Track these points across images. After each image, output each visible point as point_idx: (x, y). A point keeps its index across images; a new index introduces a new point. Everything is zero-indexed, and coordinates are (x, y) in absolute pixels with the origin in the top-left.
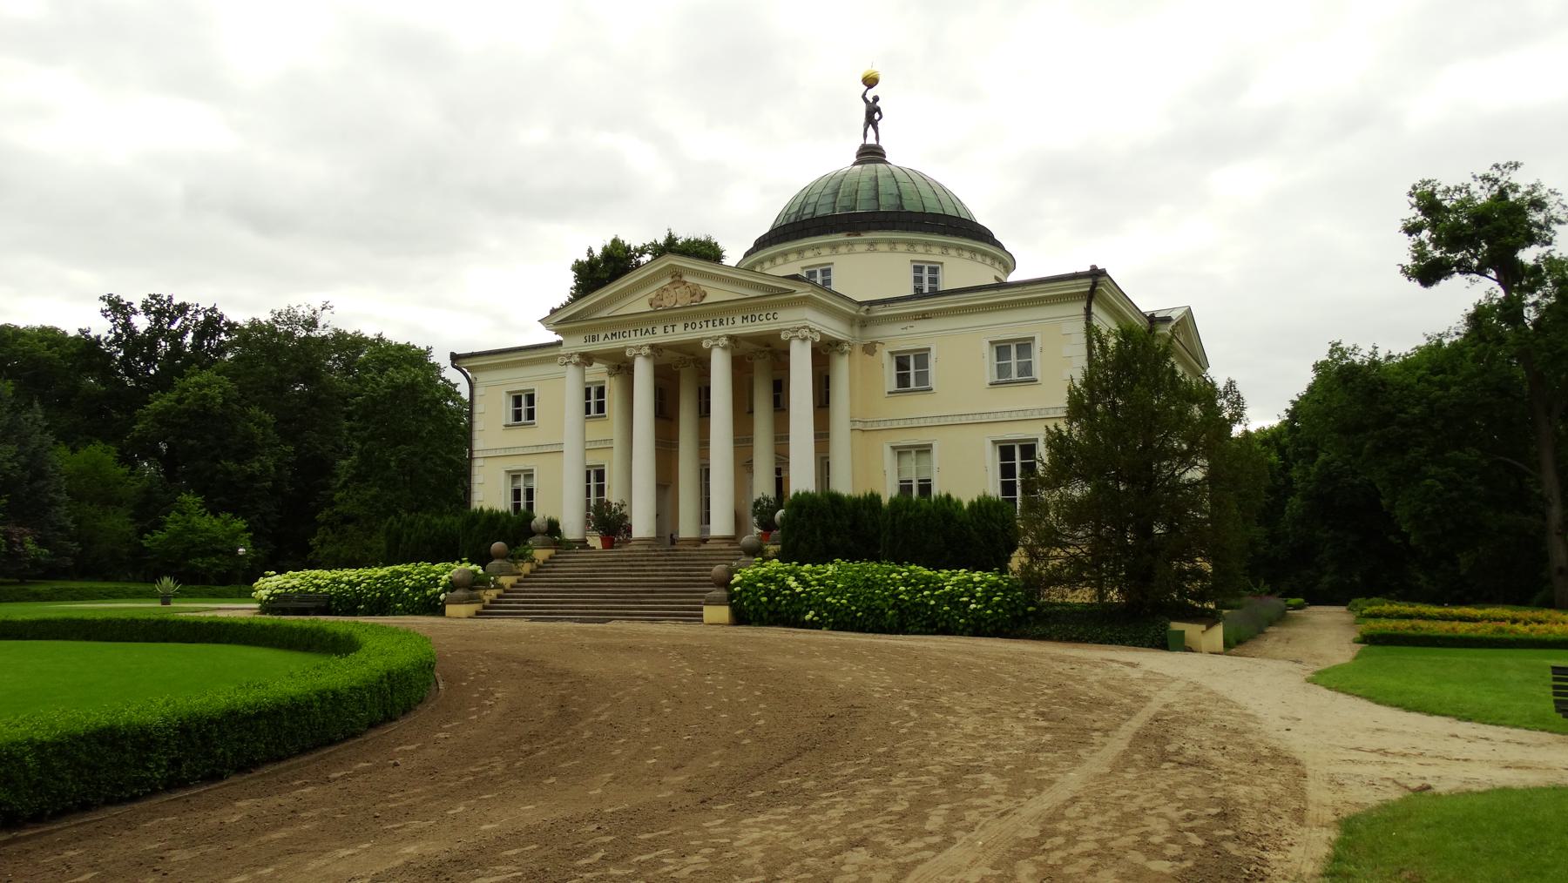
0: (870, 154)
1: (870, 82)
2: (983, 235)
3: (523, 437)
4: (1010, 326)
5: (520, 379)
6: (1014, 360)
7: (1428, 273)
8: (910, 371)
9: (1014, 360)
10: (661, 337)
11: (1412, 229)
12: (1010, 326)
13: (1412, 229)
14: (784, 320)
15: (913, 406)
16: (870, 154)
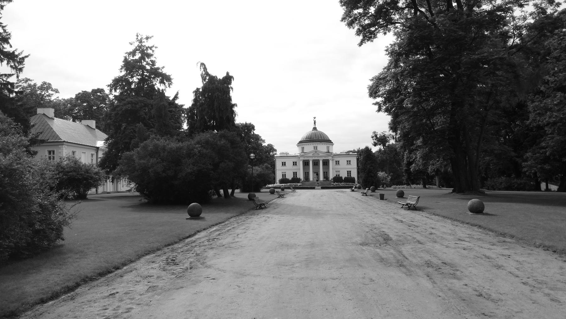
0: (315, 129)
1: (315, 118)
2: (329, 142)
3: (284, 168)
4: (349, 159)
5: (284, 160)
6: (349, 162)
7: (375, 145)
8: (337, 163)
9: (349, 162)
10: (314, 158)
11: (373, 137)
12: (349, 159)
13: (373, 137)
14: (330, 158)
15: (338, 166)
16: (315, 129)
